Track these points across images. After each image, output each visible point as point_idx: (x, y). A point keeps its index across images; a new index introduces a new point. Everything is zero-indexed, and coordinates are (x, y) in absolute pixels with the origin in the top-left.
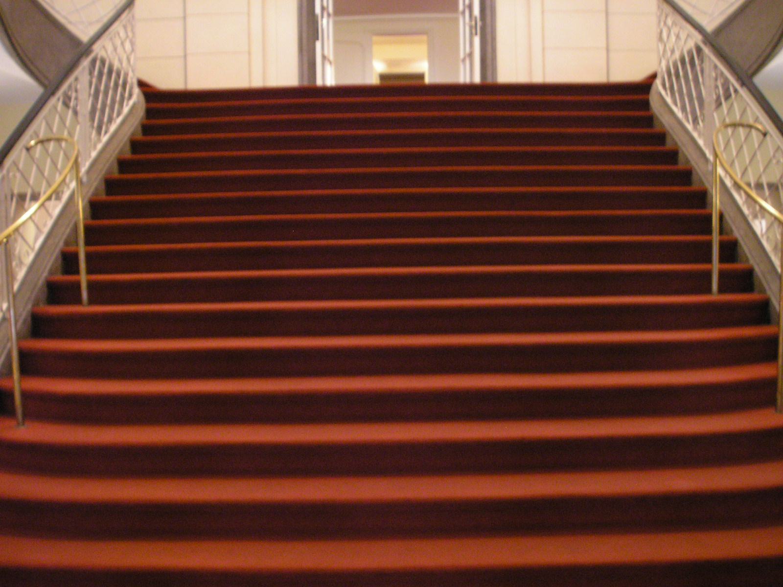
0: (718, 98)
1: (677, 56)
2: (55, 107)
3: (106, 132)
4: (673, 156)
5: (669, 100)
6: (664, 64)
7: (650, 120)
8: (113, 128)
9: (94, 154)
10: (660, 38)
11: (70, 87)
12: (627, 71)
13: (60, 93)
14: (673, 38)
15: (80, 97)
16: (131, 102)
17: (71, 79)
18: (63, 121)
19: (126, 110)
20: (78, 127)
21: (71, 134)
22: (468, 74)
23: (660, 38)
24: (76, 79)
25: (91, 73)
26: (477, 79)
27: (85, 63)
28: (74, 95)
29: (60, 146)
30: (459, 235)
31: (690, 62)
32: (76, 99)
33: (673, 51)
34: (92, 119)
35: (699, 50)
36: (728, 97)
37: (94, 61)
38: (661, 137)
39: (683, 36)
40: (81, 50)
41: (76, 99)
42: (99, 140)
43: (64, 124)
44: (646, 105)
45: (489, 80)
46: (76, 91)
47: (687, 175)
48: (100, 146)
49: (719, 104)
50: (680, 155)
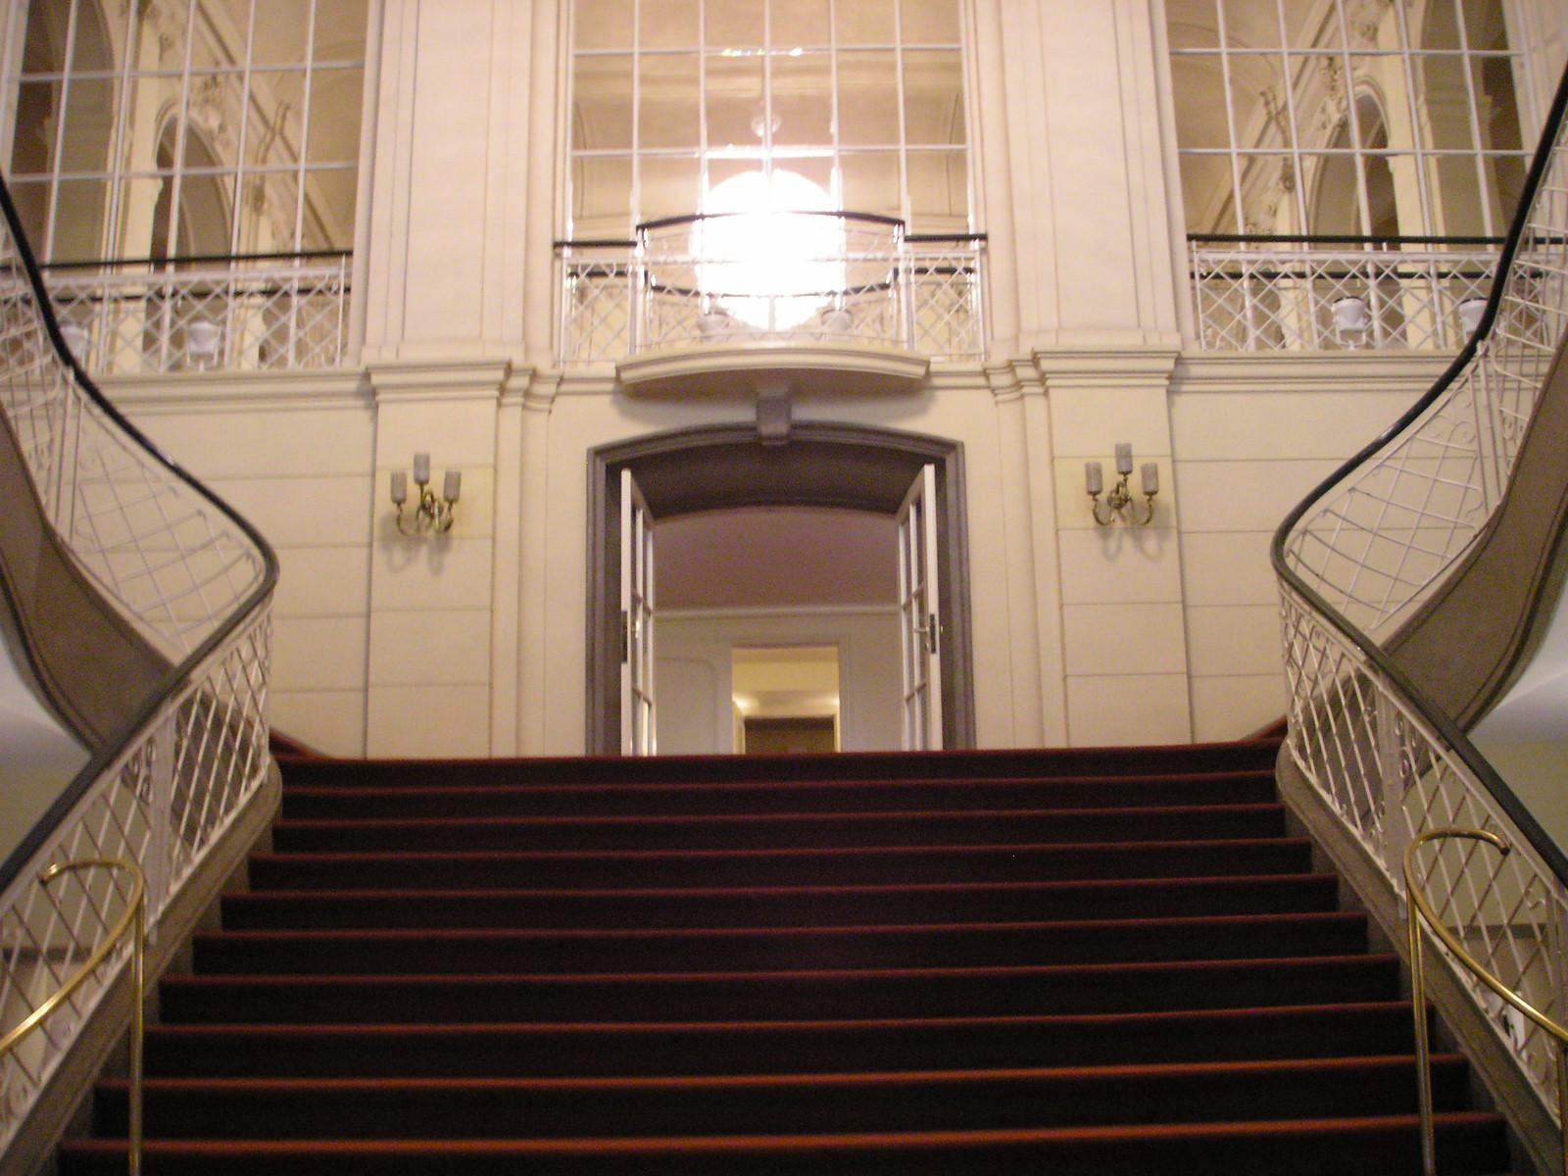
0: (1408, 771)
1: (1323, 687)
2: (105, 797)
3: (202, 842)
4: (1329, 889)
5: (1313, 779)
6: (1299, 705)
7: (1278, 819)
8: (216, 835)
9: (175, 888)
10: (1290, 659)
11: (136, 757)
12: (1226, 722)
13: (119, 765)
14: (1314, 658)
15: (154, 774)
16: (255, 784)
17: (141, 740)
18: (117, 824)
19: (244, 798)
20: (148, 836)
21: (132, 852)
22: (918, 731)
23: (1290, 659)
24: (150, 741)
25: (179, 730)
26: (936, 744)
27: (171, 709)
28: (143, 773)
29: (111, 875)
30: (612, 1133)
31: (1343, 706)
32: (147, 780)
33: (1315, 683)
34: (177, 814)
35: (1363, 681)
36: (1425, 769)
37: (185, 710)
38: (1303, 852)
39: (1333, 654)
40: (169, 679)
41: (147, 780)
42: (188, 859)
43: (120, 829)
44: (1269, 788)
45: (961, 746)
46: (149, 764)
47: (1357, 930)
48: (187, 872)
49: (1409, 783)
50: (1342, 890)
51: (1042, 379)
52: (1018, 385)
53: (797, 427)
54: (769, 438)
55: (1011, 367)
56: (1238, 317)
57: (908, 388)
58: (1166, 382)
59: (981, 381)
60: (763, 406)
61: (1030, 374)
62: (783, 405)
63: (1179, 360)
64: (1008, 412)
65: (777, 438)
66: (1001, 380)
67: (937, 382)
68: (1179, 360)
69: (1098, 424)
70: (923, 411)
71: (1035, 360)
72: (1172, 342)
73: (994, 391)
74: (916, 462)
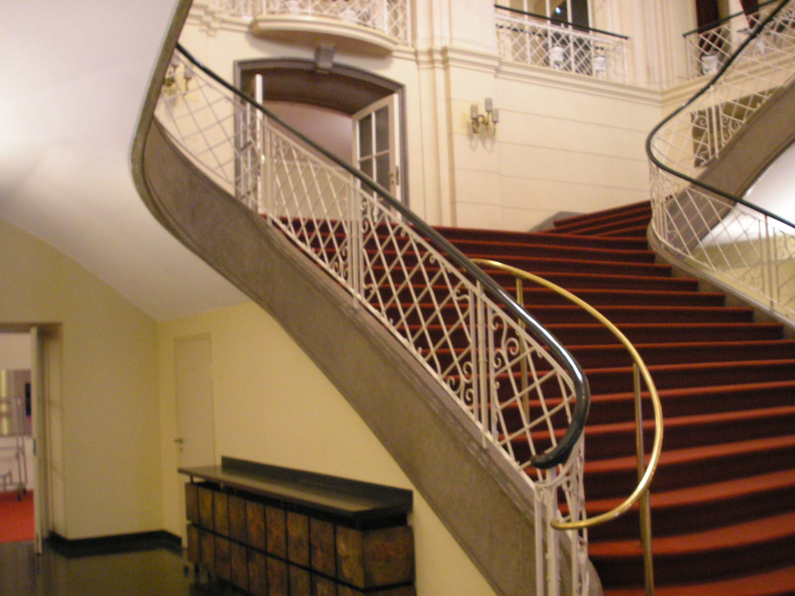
51: (445, 62)
52: (432, 62)
53: (336, 66)
54: (324, 69)
55: (430, 52)
56: (535, 51)
57: (381, 53)
58: (494, 72)
59: (413, 57)
60: (318, 51)
61: (442, 58)
62: (330, 53)
63: (501, 63)
64: (425, 74)
65: (328, 70)
66: (423, 58)
67: (395, 54)
68: (501, 63)
69: (471, 88)
70: (387, 67)
71: (444, 51)
72: (494, 52)
73: (418, 62)
74: (390, 92)
